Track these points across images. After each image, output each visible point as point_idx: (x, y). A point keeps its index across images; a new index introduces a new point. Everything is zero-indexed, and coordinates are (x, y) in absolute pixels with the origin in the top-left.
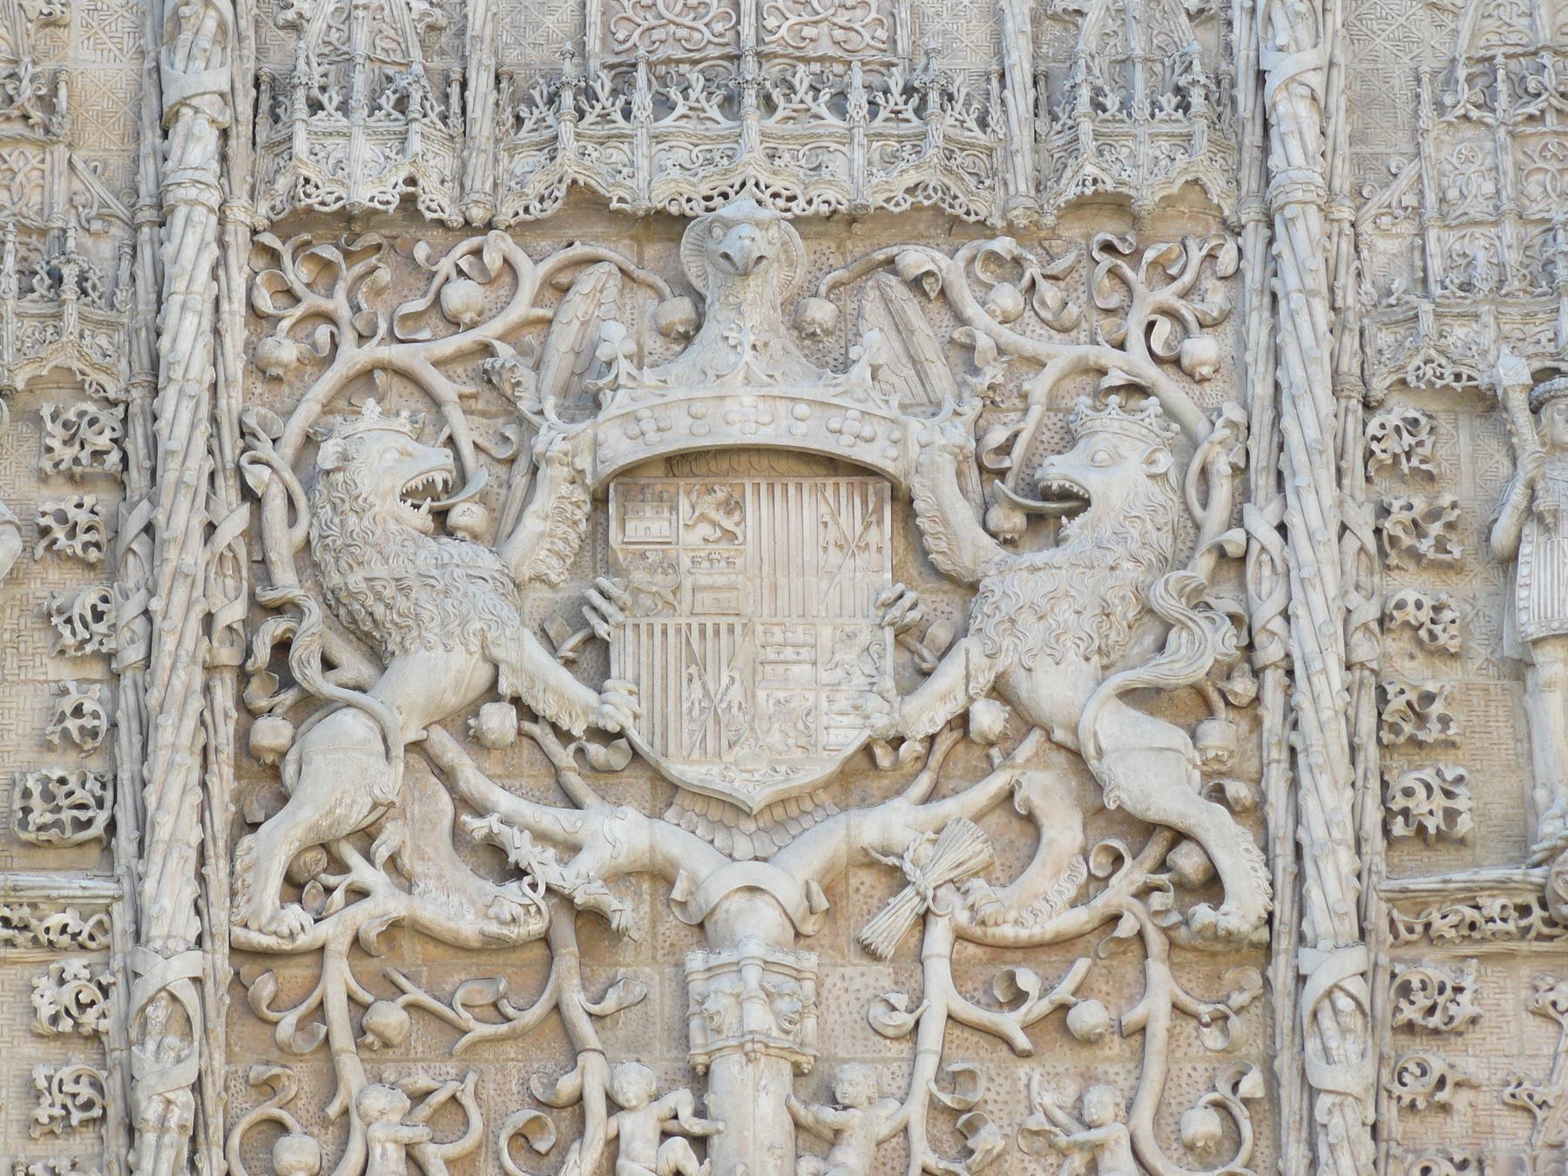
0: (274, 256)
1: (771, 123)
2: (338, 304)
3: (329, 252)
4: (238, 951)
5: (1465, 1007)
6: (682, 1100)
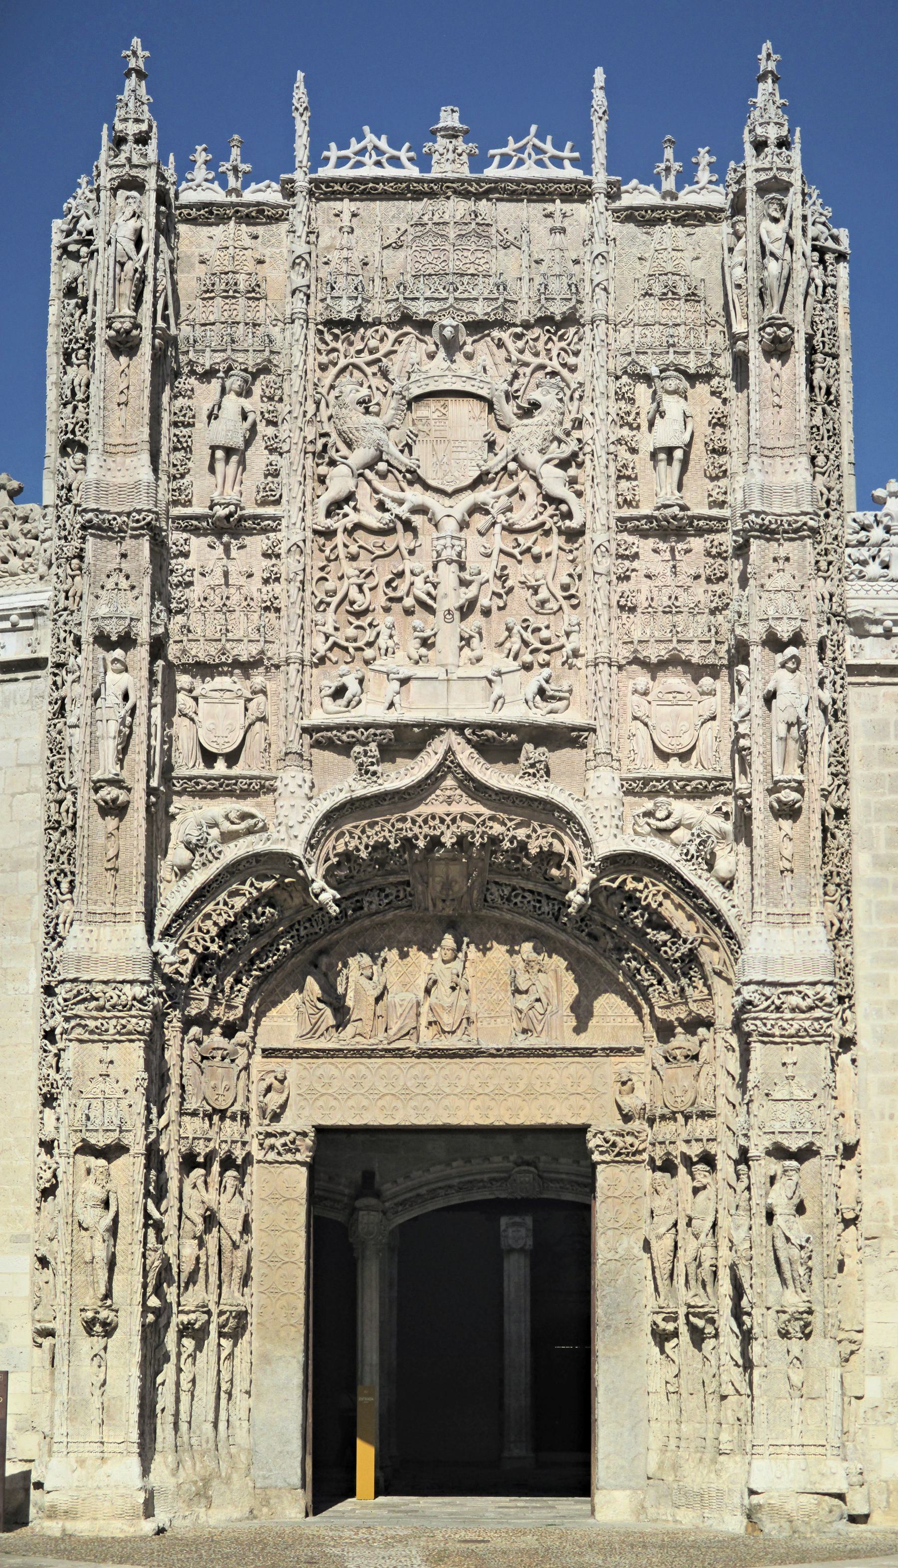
0: (321, 332)
1: (457, 294)
2: (338, 345)
3: (336, 331)
4: (316, 532)
5: (634, 550)
6: (430, 572)
